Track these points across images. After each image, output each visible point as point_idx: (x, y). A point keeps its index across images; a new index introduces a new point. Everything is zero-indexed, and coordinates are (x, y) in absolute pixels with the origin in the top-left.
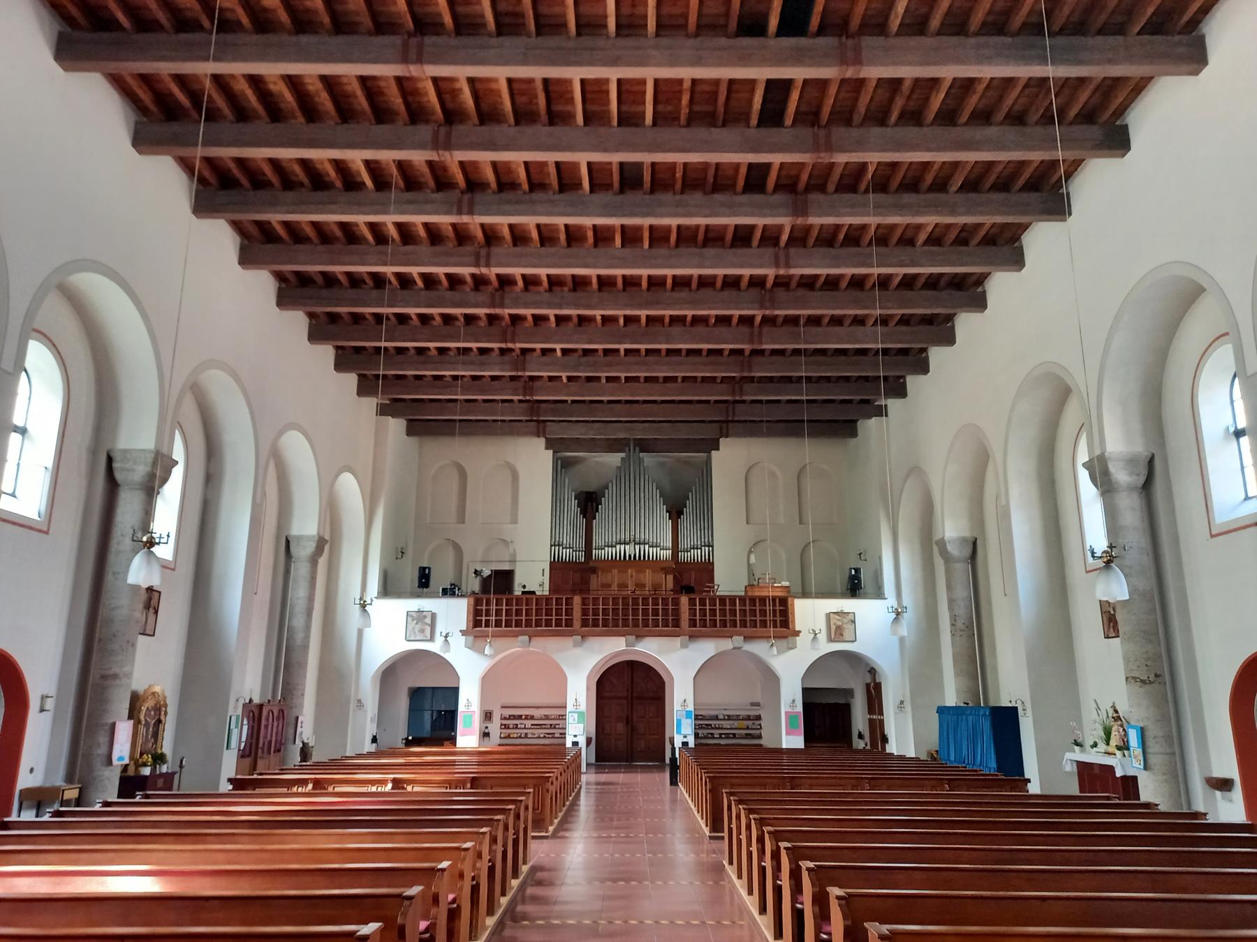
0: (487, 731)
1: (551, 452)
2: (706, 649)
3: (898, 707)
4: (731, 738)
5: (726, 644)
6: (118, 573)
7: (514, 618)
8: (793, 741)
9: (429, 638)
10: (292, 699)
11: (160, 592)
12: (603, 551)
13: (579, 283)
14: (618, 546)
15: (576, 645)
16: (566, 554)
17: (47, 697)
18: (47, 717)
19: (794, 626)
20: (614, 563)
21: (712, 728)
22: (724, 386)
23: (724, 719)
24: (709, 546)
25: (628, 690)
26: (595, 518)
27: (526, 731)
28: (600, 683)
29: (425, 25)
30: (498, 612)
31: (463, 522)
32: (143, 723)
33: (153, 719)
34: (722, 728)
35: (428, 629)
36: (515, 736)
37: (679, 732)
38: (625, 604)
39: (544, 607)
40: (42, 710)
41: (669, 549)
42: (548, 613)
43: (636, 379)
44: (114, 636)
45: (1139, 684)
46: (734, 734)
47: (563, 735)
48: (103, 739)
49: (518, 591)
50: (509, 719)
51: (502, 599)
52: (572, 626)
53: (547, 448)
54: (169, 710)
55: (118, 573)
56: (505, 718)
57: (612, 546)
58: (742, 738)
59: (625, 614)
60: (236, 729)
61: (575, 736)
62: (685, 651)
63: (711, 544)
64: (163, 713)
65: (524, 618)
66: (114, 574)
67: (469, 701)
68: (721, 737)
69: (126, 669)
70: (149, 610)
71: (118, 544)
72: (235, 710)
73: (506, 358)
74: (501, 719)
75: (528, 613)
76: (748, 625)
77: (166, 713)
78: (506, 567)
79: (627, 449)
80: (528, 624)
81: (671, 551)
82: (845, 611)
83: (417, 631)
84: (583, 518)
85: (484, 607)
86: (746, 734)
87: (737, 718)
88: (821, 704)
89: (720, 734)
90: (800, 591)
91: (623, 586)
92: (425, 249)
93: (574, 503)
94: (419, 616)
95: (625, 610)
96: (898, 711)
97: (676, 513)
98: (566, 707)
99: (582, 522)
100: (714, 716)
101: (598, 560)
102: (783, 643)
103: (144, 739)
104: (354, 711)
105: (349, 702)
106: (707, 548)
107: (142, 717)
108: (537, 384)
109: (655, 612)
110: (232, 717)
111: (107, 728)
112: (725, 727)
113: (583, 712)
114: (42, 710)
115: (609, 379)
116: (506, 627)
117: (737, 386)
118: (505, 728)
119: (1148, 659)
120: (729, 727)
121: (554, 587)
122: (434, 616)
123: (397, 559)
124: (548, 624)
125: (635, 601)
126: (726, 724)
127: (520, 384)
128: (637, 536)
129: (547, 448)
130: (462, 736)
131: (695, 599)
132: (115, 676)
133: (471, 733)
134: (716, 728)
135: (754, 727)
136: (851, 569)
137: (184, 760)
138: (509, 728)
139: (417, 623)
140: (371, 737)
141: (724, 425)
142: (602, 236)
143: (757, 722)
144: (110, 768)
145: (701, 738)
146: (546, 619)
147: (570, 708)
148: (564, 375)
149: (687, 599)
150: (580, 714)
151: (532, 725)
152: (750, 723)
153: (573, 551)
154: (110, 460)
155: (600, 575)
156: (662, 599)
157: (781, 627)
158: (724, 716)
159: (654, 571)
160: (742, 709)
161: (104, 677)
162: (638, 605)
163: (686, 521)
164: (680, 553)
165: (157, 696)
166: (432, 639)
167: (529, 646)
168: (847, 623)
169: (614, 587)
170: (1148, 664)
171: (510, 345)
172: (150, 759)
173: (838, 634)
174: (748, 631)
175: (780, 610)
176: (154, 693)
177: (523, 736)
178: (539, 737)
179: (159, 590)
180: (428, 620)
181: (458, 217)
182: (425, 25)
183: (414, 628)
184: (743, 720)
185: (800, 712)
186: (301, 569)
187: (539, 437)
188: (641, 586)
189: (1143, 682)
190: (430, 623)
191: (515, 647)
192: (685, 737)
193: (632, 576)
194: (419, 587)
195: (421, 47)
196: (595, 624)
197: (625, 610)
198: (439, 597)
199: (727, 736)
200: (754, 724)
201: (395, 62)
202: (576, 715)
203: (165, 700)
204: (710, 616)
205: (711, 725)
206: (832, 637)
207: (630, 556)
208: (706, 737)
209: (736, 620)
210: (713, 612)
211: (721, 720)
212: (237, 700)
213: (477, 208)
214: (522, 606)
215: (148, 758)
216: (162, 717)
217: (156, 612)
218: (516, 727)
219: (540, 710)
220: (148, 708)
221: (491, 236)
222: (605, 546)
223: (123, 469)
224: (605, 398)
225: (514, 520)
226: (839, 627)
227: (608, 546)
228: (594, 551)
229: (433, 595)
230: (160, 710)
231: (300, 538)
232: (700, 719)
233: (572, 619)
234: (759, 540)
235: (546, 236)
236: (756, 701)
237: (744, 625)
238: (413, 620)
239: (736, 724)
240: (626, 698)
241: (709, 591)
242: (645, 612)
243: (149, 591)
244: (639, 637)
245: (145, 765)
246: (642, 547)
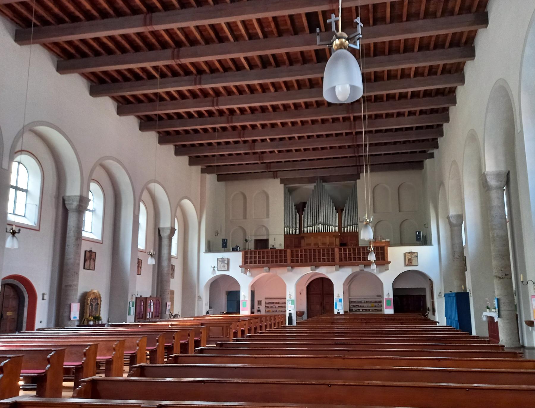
0: (259, 309)
1: (283, 185)
2: (347, 272)
3: (438, 296)
4: (367, 311)
5: (357, 269)
6: (69, 245)
7: (262, 260)
8: (389, 311)
9: (227, 269)
10: (164, 295)
11: (96, 253)
12: (307, 229)
13: (263, 109)
14: (314, 226)
15: (288, 271)
16: (291, 231)
17: (45, 294)
18: (46, 302)
19: (388, 259)
20: (311, 234)
21: (359, 307)
22: (350, 149)
23: (364, 303)
24: (356, 224)
25: (321, 291)
26: (303, 214)
27: (276, 309)
28: (309, 287)
29: (152, 9)
30: (255, 257)
31: (246, 219)
32: (89, 304)
33: (94, 303)
34: (364, 307)
35: (226, 266)
36: (272, 311)
37: (336, 308)
38: (310, 252)
39: (274, 254)
40: (43, 299)
42: (276, 257)
43: (308, 149)
44: (69, 270)
45: (498, 279)
46: (369, 310)
47: (285, 311)
48: (67, 310)
49: (270, 247)
50: (269, 304)
51: (261, 251)
52: (287, 263)
53: (281, 183)
54: (102, 299)
55: (69, 245)
56: (267, 304)
57: (311, 227)
58: (373, 311)
59: (310, 256)
60: (133, 307)
61: (290, 310)
62: (338, 272)
63: (357, 223)
64: (99, 301)
65: (266, 260)
66: (68, 246)
67: (245, 296)
68: (363, 311)
69: (75, 283)
70: (91, 260)
71: (69, 234)
72: (131, 300)
73: (246, 145)
74: (265, 304)
75: (268, 257)
77: (101, 301)
78: (265, 238)
79: (316, 181)
80: (268, 262)
82: (413, 252)
83: (222, 267)
85: (249, 255)
86: (375, 309)
87: (371, 302)
88: (414, 296)
89: (363, 309)
90: (399, 243)
91: (315, 244)
92: (191, 101)
93: (294, 207)
94: (222, 260)
95: (310, 255)
96: (438, 297)
97: (340, 210)
98: (286, 299)
100: (359, 301)
101: (305, 233)
102: (383, 268)
103: (91, 311)
104: (198, 301)
105: (195, 297)
107: (89, 302)
108: (265, 155)
109: (324, 255)
110: (130, 303)
111: (68, 306)
112: (365, 306)
113: (294, 300)
114: (43, 299)
115: (296, 150)
116: (258, 263)
117: (356, 149)
118: (267, 308)
119: (502, 267)
120: (367, 306)
121: (286, 246)
122: (228, 260)
123: (215, 236)
124: (277, 262)
125: (315, 250)
126: (365, 305)
127: (258, 155)
128: (322, 221)
129: (281, 183)
130: (242, 311)
131: (346, 249)
132: (70, 286)
133: (247, 310)
134: (360, 307)
135: (378, 306)
136: (416, 232)
137: (109, 319)
138: (269, 308)
139: (222, 263)
140: (206, 312)
141: (359, 167)
142: (264, 88)
143: (380, 304)
144: (70, 321)
145: (354, 311)
146: (276, 260)
147: (288, 298)
148: (276, 150)
150: (292, 301)
151: (279, 306)
152: (376, 304)
154: (64, 200)
155: (306, 240)
156: (327, 249)
157: (381, 260)
158: (364, 301)
159: (330, 237)
160: (373, 298)
161: (66, 286)
162: (316, 252)
163: (344, 214)
165: (95, 294)
166: (228, 270)
167: (269, 272)
168: (414, 257)
169: (313, 244)
170: (502, 269)
171: (246, 139)
172: (92, 319)
173: (409, 262)
175: (381, 252)
176: (94, 293)
177: (275, 311)
178: (282, 312)
179: (95, 252)
180: (226, 262)
181: (195, 86)
182: (152, 9)
183: (220, 265)
184: (373, 303)
185: (391, 299)
186: (165, 242)
187: (274, 178)
188: (324, 244)
189: (500, 278)
190: (227, 263)
191: (262, 273)
192: (338, 310)
193: (320, 240)
194: (222, 247)
195: (151, 18)
196: (297, 262)
197: (310, 255)
198: (231, 252)
199: (366, 310)
200: (378, 305)
201: (141, 26)
202: (290, 301)
203: (100, 295)
204: (353, 256)
205: (358, 305)
206: (407, 264)
207: (317, 230)
208: (356, 311)
209: (360, 258)
210: (350, 254)
211: (363, 303)
212: (132, 296)
213: (202, 82)
215: (92, 318)
216: (99, 302)
217: (94, 261)
218: (272, 307)
219: (282, 300)
220: (91, 299)
221: (217, 92)
222: (308, 227)
223: (68, 204)
224: (299, 159)
225: (268, 216)
226: (410, 259)
228: (303, 229)
229: (228, 251)
230: (97, 299)
231: (163, 228)
232: (353, 303)
233: (287, 260)
234: (379, 220)
235: (240, 90)
236: (379, 294)
238: (220, 262)
239: (370, 305)
240: (321, 294)
241: (352, 245)
242: (319, 255)
243: (90, 252)
244: (317, 267)
245: (90, 321)
246: (325, 226)
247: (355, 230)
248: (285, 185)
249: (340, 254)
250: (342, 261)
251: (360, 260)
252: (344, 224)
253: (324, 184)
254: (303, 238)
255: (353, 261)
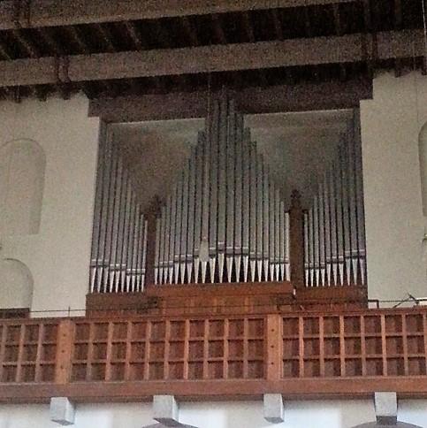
16: (114, 279)
41: (285, 263)
53: (91, 114)
57: (186, 262)
76: (406, 369)
81: (288, 266)
84: (144, 220)
99: (139, 225)
106: (355, 261)
129: (91, 114)
149: (280, 320)
153: (126, 274)
164: (307, 271)
174: (407, 382)
214: (16, 360)
227: (181, 262)
228: (156, 270)
233: (53, 366)
237: (398, 365)
247: (355, 276)
248: (106, 122)
249: (291, 340)
250: (296, 373)
251: (380, 372)
252: (316, 248)
253: (248, 120)
254: (154, 302)
255: (347, 374)
